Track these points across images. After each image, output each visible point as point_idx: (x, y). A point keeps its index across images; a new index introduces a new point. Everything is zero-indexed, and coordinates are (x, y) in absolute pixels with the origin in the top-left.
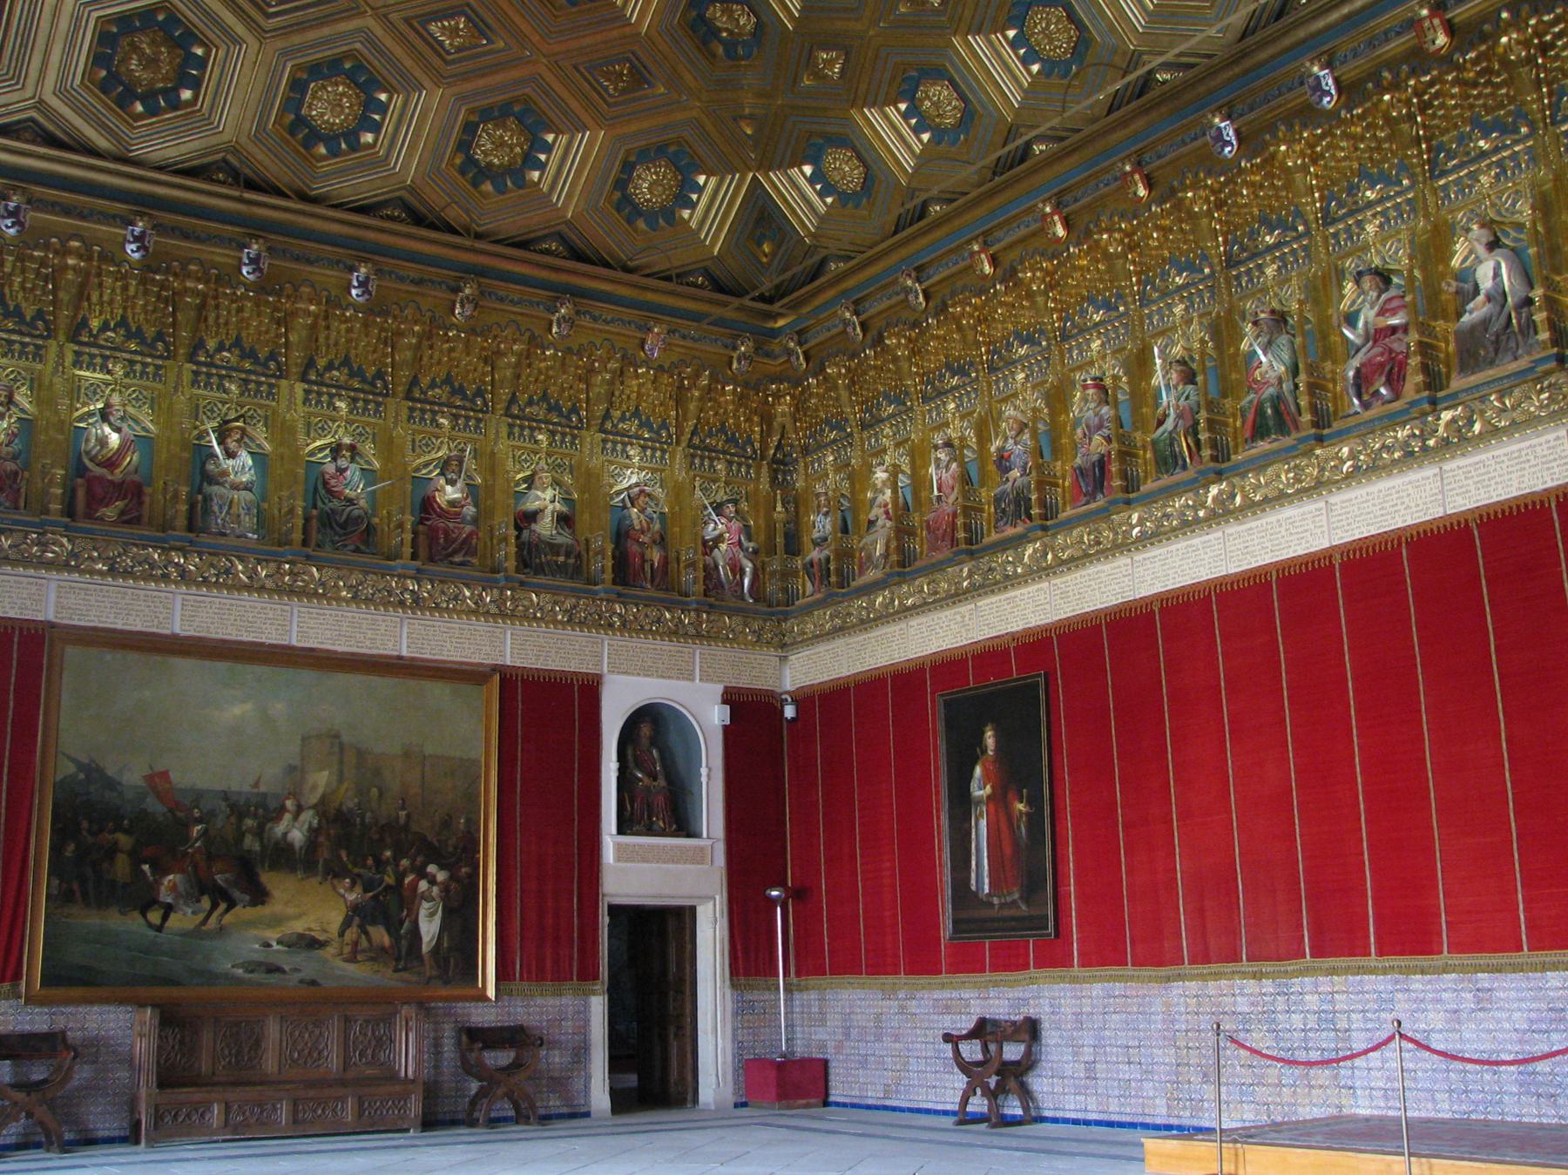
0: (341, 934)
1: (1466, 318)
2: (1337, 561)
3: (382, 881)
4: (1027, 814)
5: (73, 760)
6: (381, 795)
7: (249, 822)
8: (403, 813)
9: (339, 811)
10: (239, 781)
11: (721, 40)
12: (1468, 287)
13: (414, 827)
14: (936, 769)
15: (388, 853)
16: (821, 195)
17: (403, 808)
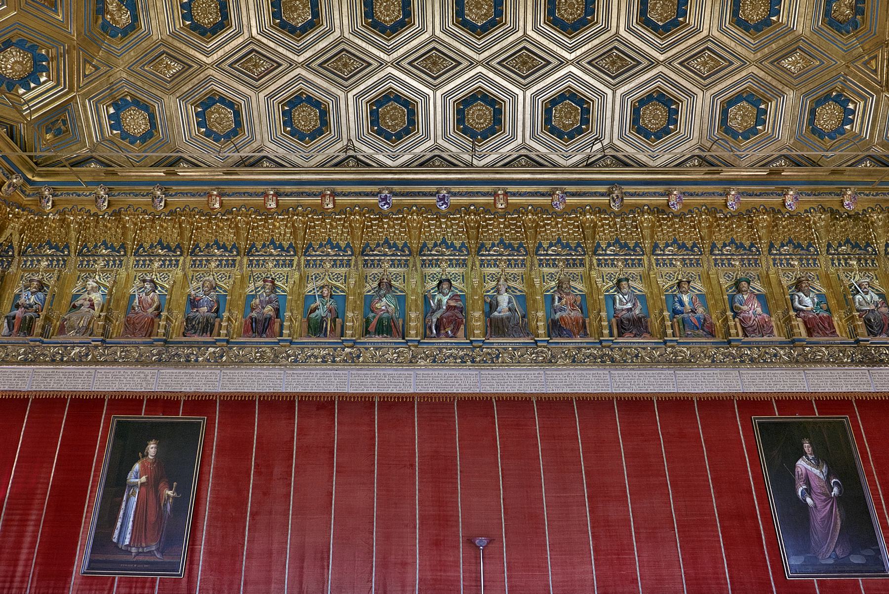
1: (496, 313)
2: (376, 400)
4: (173, 497)
11: (103, 17)
12: (495, 302)
14: (99, 461)
16: (112, 127)
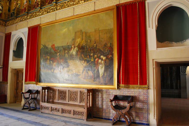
0: (83, 73)
3: (91, 60)
5: (43, 45)
6: (90, 41)
7: (66, 51)
8: (95, 45)
9: (82, 46)
10: (65, 44)
13: (98, 47)
15: (92, 54)
17: (95, 44)
